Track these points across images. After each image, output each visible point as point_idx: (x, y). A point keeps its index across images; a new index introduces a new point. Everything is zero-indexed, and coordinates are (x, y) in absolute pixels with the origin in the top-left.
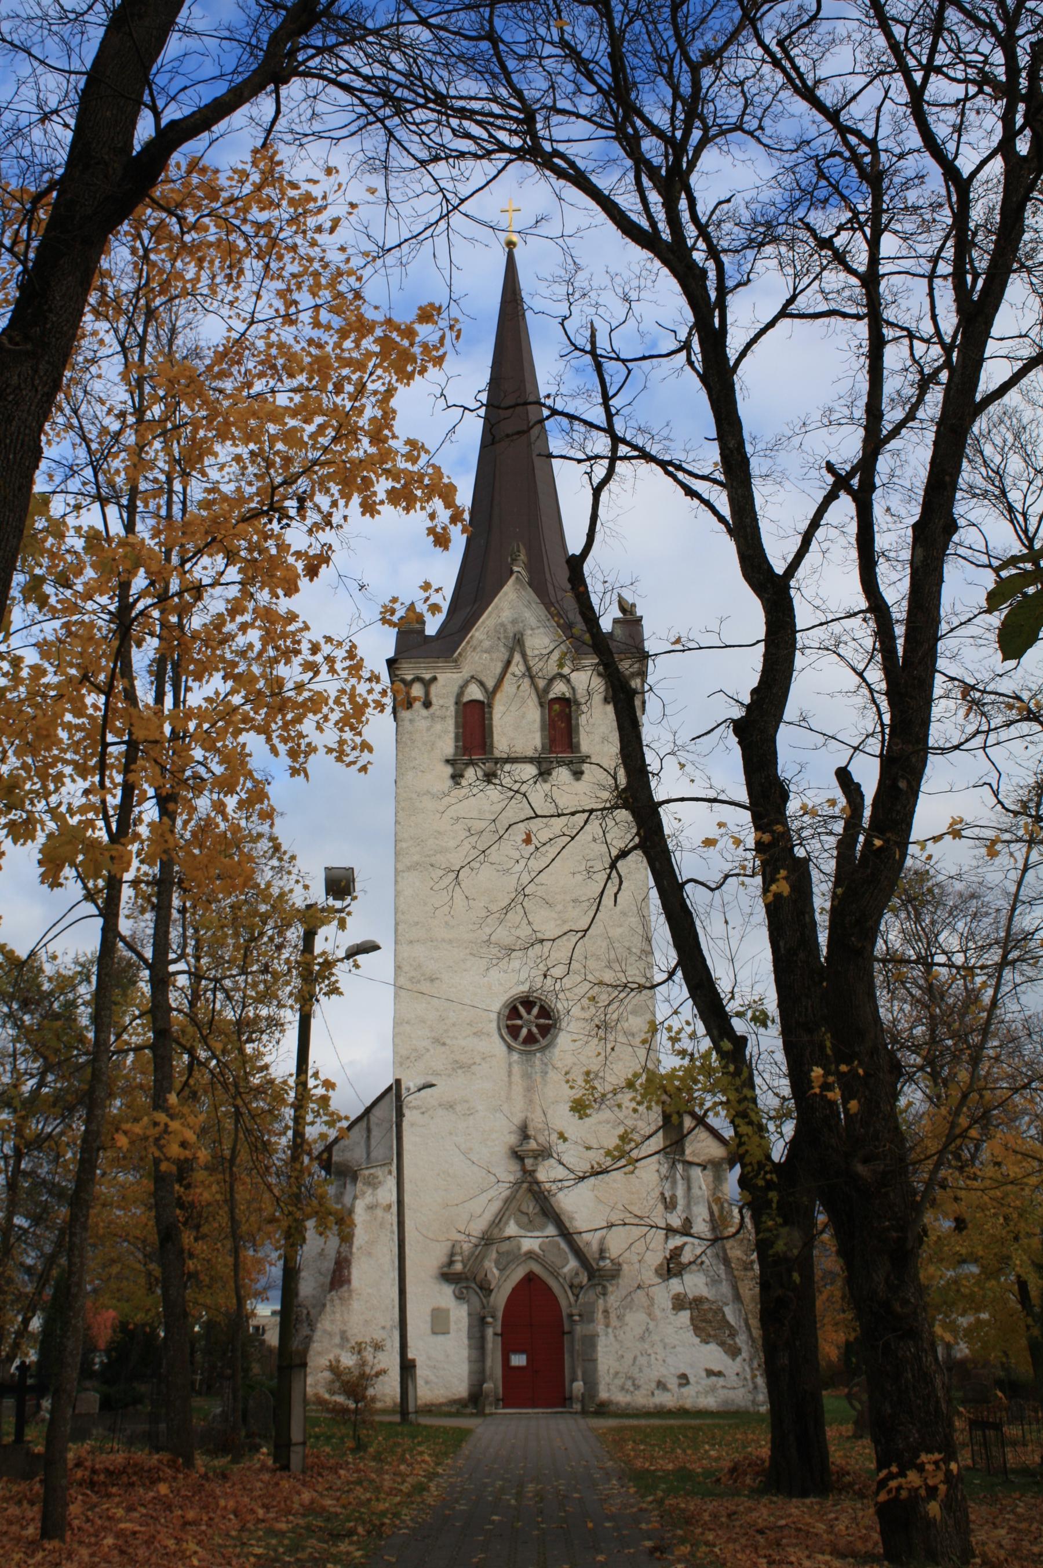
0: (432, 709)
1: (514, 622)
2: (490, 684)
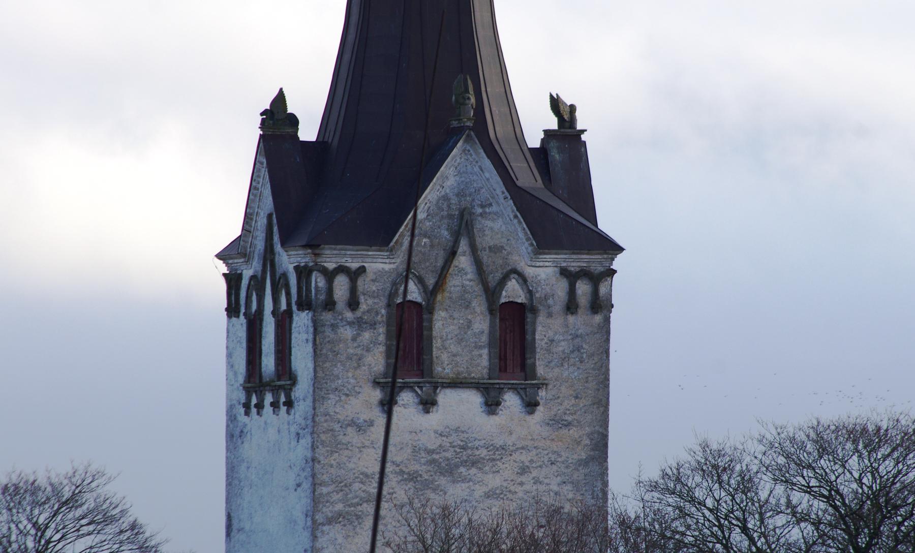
0: (358, 313)
1: (460, 194)
2: (431, 281)
